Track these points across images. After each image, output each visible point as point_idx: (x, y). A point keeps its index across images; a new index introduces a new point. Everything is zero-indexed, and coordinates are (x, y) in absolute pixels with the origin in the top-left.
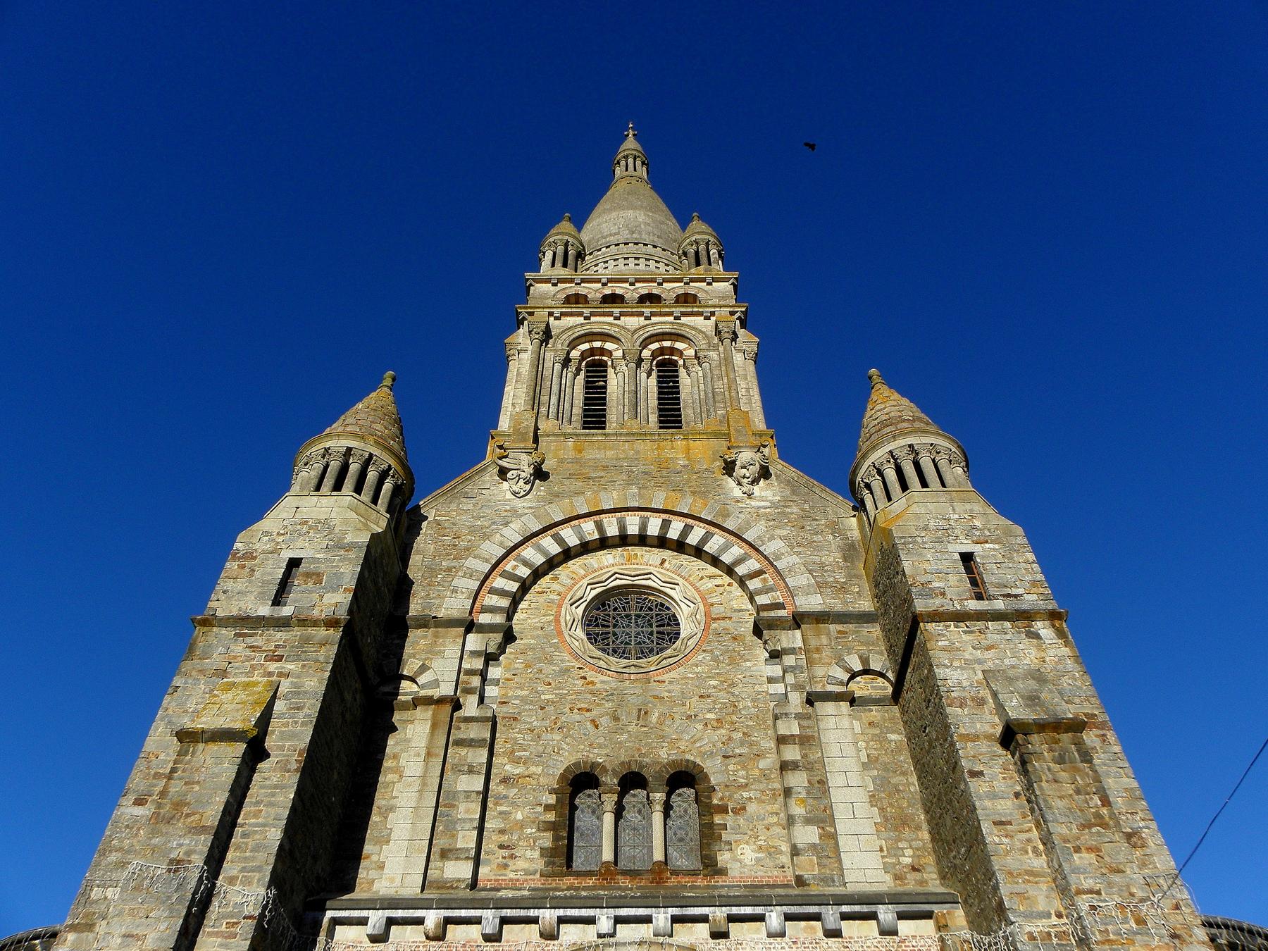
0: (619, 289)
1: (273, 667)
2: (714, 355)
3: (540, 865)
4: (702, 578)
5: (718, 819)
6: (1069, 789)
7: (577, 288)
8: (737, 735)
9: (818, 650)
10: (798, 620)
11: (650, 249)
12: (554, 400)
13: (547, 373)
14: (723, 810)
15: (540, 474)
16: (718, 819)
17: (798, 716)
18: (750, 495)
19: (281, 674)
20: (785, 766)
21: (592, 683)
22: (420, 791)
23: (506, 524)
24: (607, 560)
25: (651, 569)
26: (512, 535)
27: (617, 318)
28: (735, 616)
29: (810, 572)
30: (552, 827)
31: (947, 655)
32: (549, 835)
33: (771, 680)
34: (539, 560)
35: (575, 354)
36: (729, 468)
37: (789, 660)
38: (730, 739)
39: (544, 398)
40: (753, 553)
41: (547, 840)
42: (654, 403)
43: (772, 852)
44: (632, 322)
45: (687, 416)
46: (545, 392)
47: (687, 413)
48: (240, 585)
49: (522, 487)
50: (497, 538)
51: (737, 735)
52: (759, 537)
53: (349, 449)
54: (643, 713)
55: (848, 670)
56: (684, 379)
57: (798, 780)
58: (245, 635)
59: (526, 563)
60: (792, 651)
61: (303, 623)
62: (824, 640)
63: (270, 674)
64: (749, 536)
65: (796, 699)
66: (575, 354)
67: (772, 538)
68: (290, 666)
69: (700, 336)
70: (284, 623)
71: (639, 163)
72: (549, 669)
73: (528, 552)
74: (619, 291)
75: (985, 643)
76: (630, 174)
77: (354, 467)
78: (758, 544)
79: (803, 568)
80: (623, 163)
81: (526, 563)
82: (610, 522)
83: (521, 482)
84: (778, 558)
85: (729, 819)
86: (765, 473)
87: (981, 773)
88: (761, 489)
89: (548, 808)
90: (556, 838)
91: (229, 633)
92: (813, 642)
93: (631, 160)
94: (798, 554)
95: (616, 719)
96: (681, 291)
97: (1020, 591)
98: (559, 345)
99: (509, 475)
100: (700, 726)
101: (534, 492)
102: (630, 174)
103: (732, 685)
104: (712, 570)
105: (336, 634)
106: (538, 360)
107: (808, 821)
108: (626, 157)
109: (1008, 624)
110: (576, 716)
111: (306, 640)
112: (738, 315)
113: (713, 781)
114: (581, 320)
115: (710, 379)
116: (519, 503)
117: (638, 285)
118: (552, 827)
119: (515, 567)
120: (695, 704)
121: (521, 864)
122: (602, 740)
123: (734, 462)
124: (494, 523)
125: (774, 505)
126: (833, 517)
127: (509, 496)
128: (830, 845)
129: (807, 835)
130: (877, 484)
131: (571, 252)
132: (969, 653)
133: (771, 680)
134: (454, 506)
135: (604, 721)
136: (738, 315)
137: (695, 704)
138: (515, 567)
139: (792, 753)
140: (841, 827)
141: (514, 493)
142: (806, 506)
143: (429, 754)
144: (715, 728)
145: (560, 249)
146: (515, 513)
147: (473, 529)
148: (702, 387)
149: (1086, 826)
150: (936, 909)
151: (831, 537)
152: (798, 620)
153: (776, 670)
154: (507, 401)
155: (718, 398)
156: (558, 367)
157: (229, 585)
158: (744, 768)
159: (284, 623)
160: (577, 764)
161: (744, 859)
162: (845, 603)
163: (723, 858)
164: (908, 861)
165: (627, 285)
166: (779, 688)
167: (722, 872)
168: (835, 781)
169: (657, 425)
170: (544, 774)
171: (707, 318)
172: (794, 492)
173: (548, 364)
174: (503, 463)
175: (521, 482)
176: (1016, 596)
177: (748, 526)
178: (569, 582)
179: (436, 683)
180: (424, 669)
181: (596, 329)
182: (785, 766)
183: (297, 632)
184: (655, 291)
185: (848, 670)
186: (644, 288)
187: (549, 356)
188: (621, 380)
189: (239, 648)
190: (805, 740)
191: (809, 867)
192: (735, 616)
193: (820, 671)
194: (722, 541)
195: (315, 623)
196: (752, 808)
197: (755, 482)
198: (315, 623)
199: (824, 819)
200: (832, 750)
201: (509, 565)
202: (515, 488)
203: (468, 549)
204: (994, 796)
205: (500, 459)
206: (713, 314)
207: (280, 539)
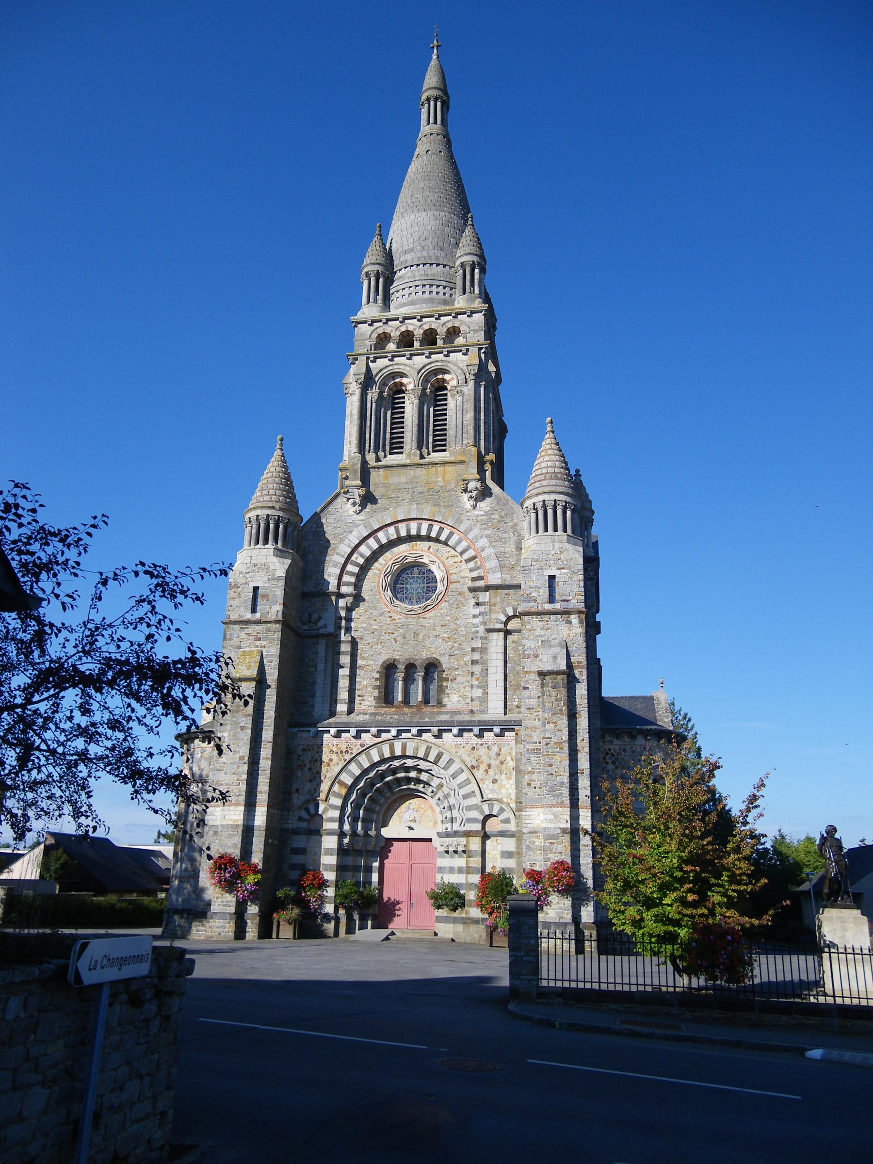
1: (258, 643)
3: (374, 703)
5: (444, 684)
6: (553, 699)
7: (385, 327)
8: (456, 645)
9: (495, 605)
10: (488, 588)
14: (447, 680)
16: (444, 684)
17: (482, 638)
19: (261, 647)
20: (474, 662)
21: (394, 619)
22: (325, 663)
23: (351, 532)
24: (402, 550)
25: (423, 553)
28: (462, 580)
30: (378, 687)
31: (529, 633)
32: (377, 691)
33: (474, 617)
37: (482, 609)
38: (453, 647)
41: (376, 693)
43: (464, 697)
47: (451, 433)
48: (236, 602)
50: (347, 541)
51: (456, 645)
52: (476, 536)
53: (268, 515)
54: (416, 635)
55: (506, 615)
57: (477, 669)
58: (243, 628)
59: (362, 555)
60: (483, 604)
61: (266, 622)
62: (498, 599)
63: (257, 647)
65: (481, 629)
67: (481, 538)
68: (264, 643)
70: (258, 622)
72: (375, 613)
74: (411, 328)
75: (546, 626)
77: (272, 526)
80: (426, 105)
81: (362, 555)
85: (449, 684)
87: (528, 688)
89: (376, 679)
90: (380, 693)
91: (237, 627)
92: (493, 601)
93: (432, 103)
94: (494, 546)
95: (404, 638)
96: (450, 325)
97: (570, 598)
100: (440, 641)
103: (457, 619)
104: (453, 552)
105: (278, 626)
107: (479, 687)
109: (559, 616)
110: (387, 637)
111: (268, 630)
113: (444, 667)
118: (378, 687)
120: (439, 630)
121: (367, 703)
122: (398, 648)
126: (515, 521)
128: (484, 699)
129: (478, 693)
132: (539, 632)
133: (474, 617)
135: (399, 639)
136: (483, 350)
137: (439, 630)
139: (477, 656)
140: (490, 691)
142: (503, 514)
143: (326, 660)
144: (447, 642)
149: (554, 714)
150: (516, 728)
152: (488, 588)
153: (476, 611)
155: (465, 430)
157: (231, 602)
158: (458, 660)
159: (258, 622)
160: (388, 660)
161: (453, 700)
162: (512, 577)
163: (445, 700)
164: (516, 703)
166: (477, 621)
167: (445, 706)
168: (491, 670)
170: (374, 664)
171: (464, 354)
176: (567, 601)
178: (384, 562)
179: (325, 626)
180: (320, 618)
181: (396, 368)
182: (474, 662)
183: (264, 626)
185: (506, 615)
189: (243, 634)
190: (483, 650)
191: (476, 705)
192: (462, 580)
193: (494, 616)
194: (458, 537)
195: (270, 622)
196: (459, 679)
198: (270, 622)
199: (484, 686)
200: (493, 656)
204: (530, 698)
207: (247, 575)
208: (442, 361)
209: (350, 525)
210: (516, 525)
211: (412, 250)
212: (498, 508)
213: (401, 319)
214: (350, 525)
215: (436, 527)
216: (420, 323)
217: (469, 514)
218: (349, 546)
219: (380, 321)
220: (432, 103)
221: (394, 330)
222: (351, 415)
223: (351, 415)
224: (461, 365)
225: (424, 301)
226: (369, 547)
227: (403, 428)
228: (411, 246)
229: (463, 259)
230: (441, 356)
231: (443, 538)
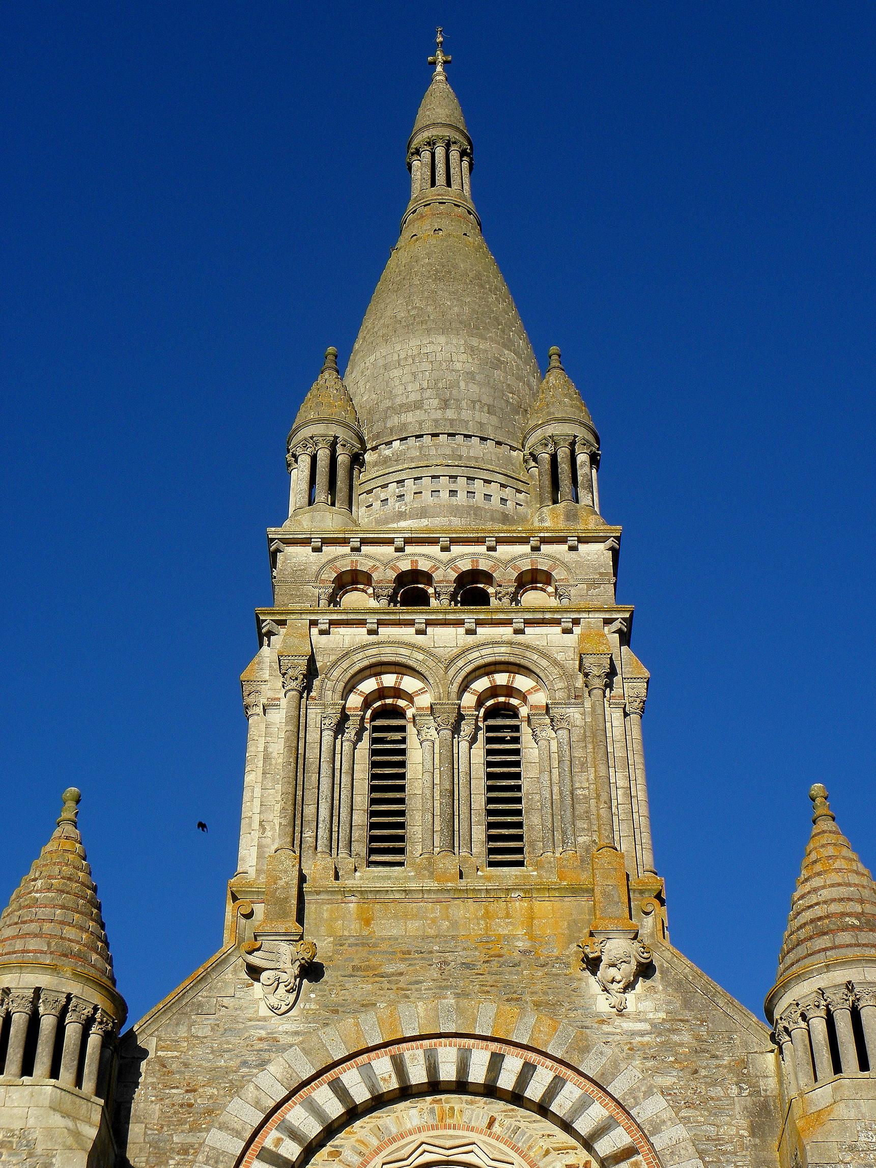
0: (423, 557)
2: (574, 713)
4: (547, 1152)
7: (355, 557)
11: (475, 448)
12: (324, 812)
13: (312, 755)
15: (311, 971)
18: (620, 1012)
23: (263, 1064)
25: (473, 1136)
26: (271, 1084)
27: (420, 632)
29: (701, 1154)
34: (313, 1129)
35: (355, 701)
36: (593, 964)
39: (309, 810)
40: (622, 1117)
42: (479, 801)
44: (446, 638)
45: (531, 828)
46: (310, 797)
47: (534, 822)
49: (282, 997)
50: (250, 1091)
52: (632, 1091)
53: (37, 991)
56: (530, 750)
59: (294, 1135)
64: (617, 1088)
66: (355, 701)
67: (649, 1093)
69: (556, 671)
71: (454, 155)
73: (297, 1115)
76: (438, 229)
77: (47, 1023)
78: (629, 1102)
79: (691, 1149)
80: (426, 155)
81: (294, 1135)
82: (414, 1058)
83: (282, 989)
84: (656, 1130)
86: (646, 970)
88: (638, 998)
93: (440, 152)
94: (685, 1120)
98: (328, 688)
99: (264, 976)
101: (300, 1004)
102: (438, 229)
104: (563, 1137)
106: (299, 725)
108: (431, 143)
112: (616, 625)
114: (359, 634)
115: (570, 766)
116: (283, 1026)
117: (456, 549)
119: (278, 1142)
123: (598, 960)
124: (245, 1063)
125: (656, 1028)
126: (740, 1053)
127: (264, 1011)
130: (799, 1033)
131: (342, 459)
134: (182, 1032)
136: (616, 625)
138: (278, 1142)
141: (272, 1009)
142: (703, 1031)
145: (323, 455)
146: (274, 1044)
147: (216, 1075)
148: (555, 772)
151: (734, 1090)
154: (251, 807)
155: (580, 809)
156: (328, 736)
165: (434, 550)
169: (483, 859)
172: (686, 1004)
173: (313, 736)
174: (256, 959)
175: (282, 989)
177: (615, 1069)
181: (388, 654)
184: (483, 565)
186: (466, 557)
187: (314, 714)
188: (428, 757)
194: (577, 1093)
197: (629, 986)
201: (269, 1139)
202: (273, 1001)
203: (210, 1112)
205: (250, 953)
206: (576, 622)
208: (510, 643)
209: (264, 1045)
210: (744, 1063)
211: (418, 405)
212: (687, 1015)
213: (399, 543)
214: (264, 1045)
215: (513, 1064)
216: (445, 556)
217: (606, 1028)
218: (257, 1105)
219: (345, 542)
220: (440, 152)
221: (382, 562)
222: (267, 757)
223: (267, 757)
224: (560, 657)
225: (455, 511)
226: (315, 1110)
227: (402, 801)
228: (413, 397)
229: (550, 430)
230: (506, 632)
231: (535, 1092)
